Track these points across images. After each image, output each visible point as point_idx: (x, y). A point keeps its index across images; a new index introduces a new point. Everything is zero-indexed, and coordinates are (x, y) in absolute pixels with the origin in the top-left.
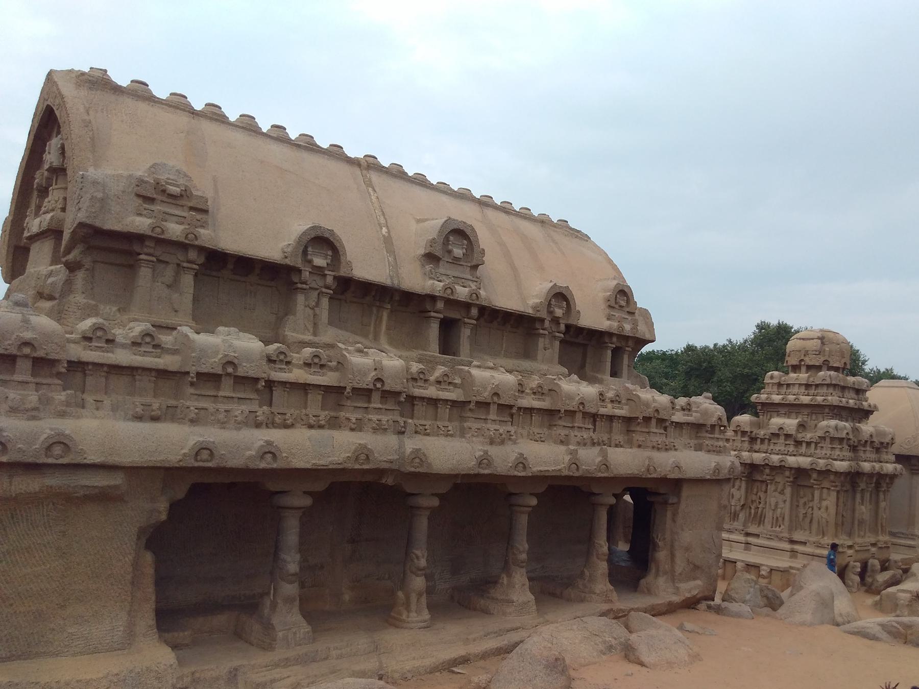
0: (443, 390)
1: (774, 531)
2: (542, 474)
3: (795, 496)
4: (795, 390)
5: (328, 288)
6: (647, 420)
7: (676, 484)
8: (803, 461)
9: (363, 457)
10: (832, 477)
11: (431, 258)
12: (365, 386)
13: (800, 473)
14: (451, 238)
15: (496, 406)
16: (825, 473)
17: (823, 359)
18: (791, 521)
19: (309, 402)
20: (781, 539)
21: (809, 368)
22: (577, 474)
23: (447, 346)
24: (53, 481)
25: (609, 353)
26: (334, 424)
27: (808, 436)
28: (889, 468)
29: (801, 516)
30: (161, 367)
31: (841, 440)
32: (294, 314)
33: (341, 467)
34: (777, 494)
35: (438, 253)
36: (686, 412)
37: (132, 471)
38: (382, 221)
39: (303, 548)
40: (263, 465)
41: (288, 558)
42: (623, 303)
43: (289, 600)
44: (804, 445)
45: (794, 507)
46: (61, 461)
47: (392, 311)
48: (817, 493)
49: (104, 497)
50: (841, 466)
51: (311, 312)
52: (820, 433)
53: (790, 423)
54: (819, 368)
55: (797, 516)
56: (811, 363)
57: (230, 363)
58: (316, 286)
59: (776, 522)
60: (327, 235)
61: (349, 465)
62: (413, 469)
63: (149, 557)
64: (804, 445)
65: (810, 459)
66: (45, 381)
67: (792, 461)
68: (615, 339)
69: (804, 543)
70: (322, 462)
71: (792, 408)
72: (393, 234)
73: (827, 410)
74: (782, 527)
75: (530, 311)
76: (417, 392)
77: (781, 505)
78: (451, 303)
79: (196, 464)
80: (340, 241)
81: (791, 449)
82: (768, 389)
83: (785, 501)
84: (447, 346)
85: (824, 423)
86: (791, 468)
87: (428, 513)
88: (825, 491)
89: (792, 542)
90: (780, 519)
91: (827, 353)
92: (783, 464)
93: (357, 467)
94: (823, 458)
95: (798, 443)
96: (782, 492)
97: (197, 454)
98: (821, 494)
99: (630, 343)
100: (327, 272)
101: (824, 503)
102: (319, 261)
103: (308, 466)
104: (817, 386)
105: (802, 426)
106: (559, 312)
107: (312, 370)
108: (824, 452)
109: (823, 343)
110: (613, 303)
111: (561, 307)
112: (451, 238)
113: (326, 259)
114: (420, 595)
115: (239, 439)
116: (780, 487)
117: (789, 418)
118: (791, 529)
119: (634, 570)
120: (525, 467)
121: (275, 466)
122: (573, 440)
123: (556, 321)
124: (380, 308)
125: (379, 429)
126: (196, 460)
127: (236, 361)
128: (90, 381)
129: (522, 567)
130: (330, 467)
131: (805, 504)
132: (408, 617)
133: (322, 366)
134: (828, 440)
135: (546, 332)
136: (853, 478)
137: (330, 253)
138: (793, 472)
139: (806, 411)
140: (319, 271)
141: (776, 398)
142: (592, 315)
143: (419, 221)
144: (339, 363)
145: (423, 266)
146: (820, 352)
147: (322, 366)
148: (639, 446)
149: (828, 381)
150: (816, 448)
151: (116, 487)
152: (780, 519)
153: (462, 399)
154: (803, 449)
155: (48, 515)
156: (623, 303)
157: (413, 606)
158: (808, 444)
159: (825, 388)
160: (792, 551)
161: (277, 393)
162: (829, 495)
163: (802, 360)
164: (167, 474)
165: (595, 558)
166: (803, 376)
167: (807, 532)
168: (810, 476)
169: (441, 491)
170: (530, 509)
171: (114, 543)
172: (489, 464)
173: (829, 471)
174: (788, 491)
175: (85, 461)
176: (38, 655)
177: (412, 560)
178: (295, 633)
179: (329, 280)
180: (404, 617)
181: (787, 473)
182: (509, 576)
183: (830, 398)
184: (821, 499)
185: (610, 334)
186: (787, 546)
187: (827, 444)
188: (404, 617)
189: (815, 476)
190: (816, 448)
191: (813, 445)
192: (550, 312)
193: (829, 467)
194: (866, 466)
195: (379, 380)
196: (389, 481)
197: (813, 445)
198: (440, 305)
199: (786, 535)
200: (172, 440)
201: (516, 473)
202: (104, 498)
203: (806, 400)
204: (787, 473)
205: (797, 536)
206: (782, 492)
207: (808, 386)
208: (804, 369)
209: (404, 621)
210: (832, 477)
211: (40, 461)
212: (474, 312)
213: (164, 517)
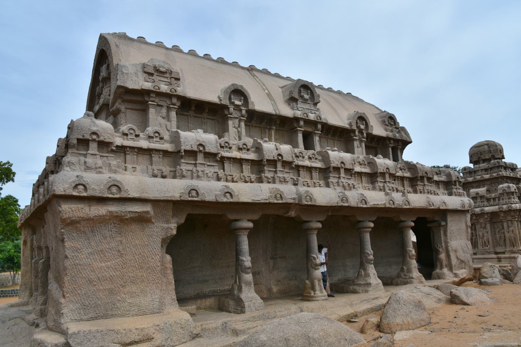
0: (313, 162)
1: (484, 249)
2: (375, 206)
3: (493, 229)
4: (480, 173)
5: (243, 117)
6: (422, 178)
7: (443, 213)
9: (279, 196)
10: (512, 214)
12: (272, 158)
13: (493, 214)
14: (302, 89)
15: (343, 169)
17: (491, 155)
18: (493, 242)
19: (244, 170)
20: (489, 253)
21: (484, 161)
22: (393, 207)
23: (308, 145)
24: (114, 208)
25: (390, 149)
29: (498, 239)
30: (165, 149)
32: (228, 131)
33: (267, 201)
34: (482, 229)
35: (296, 96)
36: (439, 175)
37: (155, 203)
38: (264, 87)
39: (251, 252)
40: (225, 200)
41: (244, 259)
42: (392, 123)
43: (248, 284)
44: (492, 200)
45: (494, 234)
46: (116, 196)
47: (276, 130)
48: (505, 225)
49: (142, 220)
51: (236, 130)
52: (500, 192)
53: (482, 190)
54: (489, 160)
55: (496, 239)
56: (484, 158)
57: (201, 145)
58: (237, 116)
59: (485, 244)
60: (240, 88)
61: (272, 201)
62: (306, 203)
63: (168, 257)
64: (492, 200)
65: (497, 207)
66: (104, 155)
67: (487, 209)
68: (392, 142)
69: (504, 253)
70: (257, 199)
72: (271, 92)
73: (500, 180)
74: (489, 246)
76: (301, 163)
77: (486, 235)
78: (308, 122)
79: (190, 199)
80: (246, 91)
81: (486, 203)
83: (487, 232)
85: (501, 186)
86: (487, 213)
87: (316, 232)
88: (509, 222)
89: (496, 253)
90: (487, 242)
91: (492, 151)
92: (483, 211)
93: (276, 201)
94: (505, 204)
95: (488, 200)
96: (485, 228)
97: (189, 193)
98: (508, 224)
99: (400, 143)
100: (242, 108)
101: (511, 229)
102: (237, 102)
103: (250, 201)
104: (491, 169)
105: (488, 190)
106: (362, 127)
107: (244, 151)
108: (504, 201)
109: (489, 147)
110: (387, 123)
111: (363, 124)
112: (302, 89)
113: (241, 101)
114: (319, 281)
115: (210, 187)
116: (483, 225)
117: (479, 188)
118: (494, 247)
120: (366, 203)
121: (232, 200)
122: (387, 188)
123: (361, 131)
124: (270, 129)
125: (284, 181)
126: (189, 197)
127: (203, 144)
128: (128, 157)
129: (371, 264)
130: (262, 201)
131: (499, 231)
132: (314, 294)
133: (248, 150)
134: (505, 194)
135: (357, 138)
137: (242, 98)
138: (489, 215)
140: (237, 108)
142: (378, 130)
144: (256, 148)
145: (289, 104)
147: (248, 150)
148: (421, 192)
149: (497, 165)
150: (499, 200)
151: (147, 212)
152: (487, 242)
153: (324, 167)
154: (492, 202)
155: (111, 231)
156: (392, 123)
157: (317, 287)
158: (494, 199)
159: (496, 168)
160: (498, 258)
161: (226, 165)
162: (512, 224)
163: (479, 158)
164: (176, 205)
165: (408, 259)
166: (483, 165)
167: (503, 247)
168: (499, 216)
169: (321, 220)
170: (371, 229)
171: (149, 245)
172: (347, 200)
173: (510, 210)
174: (488, 226)
175: (129, 196)
176: (113, 316)
177: (311, 261)
178: (254, 303)
179: (244, 112)
180: (312, 294)
181: (486, 216)
182: (365, 270)
183: (500, 173)
184: (508, 227)
186: (494, 256)
187: (506, 196)
188: (312, 294)
189: (502, 215)
190: (499, 200)
191: (497, 199)
192: (358, 127)
193: (510, 208)
195: (279, 155)
196: (293, 214)
197: (497, 199)
198: (302, 123)
199: (492, 250)
200: (174, 188)
201: (362, 206)
202: (142, 220)
203: (487, 176)
204: (486, 216)
205: (499, 250)
206: (485, 228)
207: (486, 170)
208: (481, 162)
209: (313, 297)
210: (512, 214)
211: (105, 196)
212: (319, 126)
213: (174, 232)
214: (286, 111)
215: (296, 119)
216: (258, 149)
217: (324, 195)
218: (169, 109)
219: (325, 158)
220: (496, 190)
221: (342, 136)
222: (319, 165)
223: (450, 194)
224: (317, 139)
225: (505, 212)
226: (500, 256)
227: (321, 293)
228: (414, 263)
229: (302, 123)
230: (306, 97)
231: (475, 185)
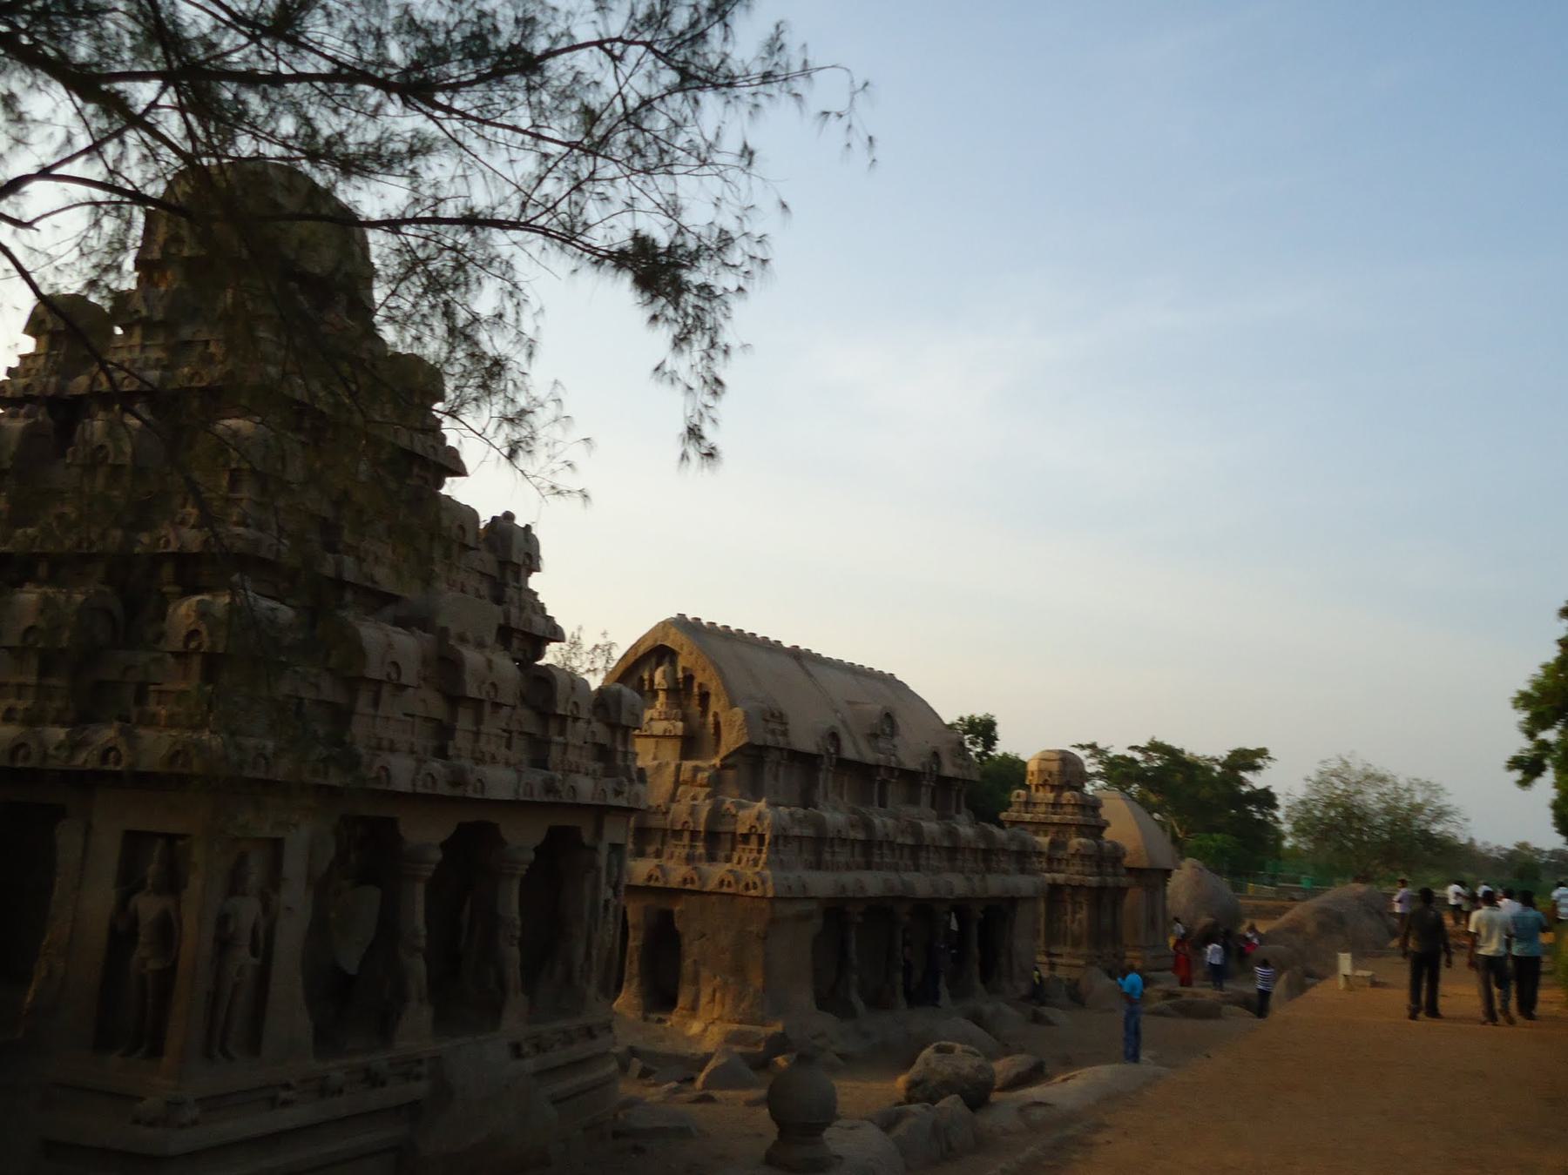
7: (1013, 901)
8: (1060, 878)
11: (875, 736)
16: (1077, 889)
26: (868, 866)
27: (1060, 854)
28: (1124, 881)
31: (1090, 857)
48: (1069, 908)
50: (1093, 881)
71: (1040, 826)
75: (919, 768)
78: (890, 770)
82: (1015, 808)
84: (882, 804)
89: (1049, 955)
105: (1053, 844)
119: (987, 972)
136: (1101, 889)
139: (1055, 829)
141: (1027, 817)
143: (849, 703)
146: (1062, 772)
154: (1055, 865)
158: (1059, 860)
184: (1074, 913)
185: (956, 779)
187: (1077, 861)
194: (1110, 881)
200: (823, 883)
203: (1056, 818)
205: (1054, 950)
214: (870, 757)
215: (878, 766)
216: (868, 826)
217: (921, 884)
218: (779, 764)
219: (916, 831)
220: (1064, 846)
221: (911, 778)
222: (910, 841)
223: (1023, 871)
224: (890, 788)
225: (1074, 887)
226: (1055, 960)
227: (901, 1001)
228: (976, 969)
229: (882, 771)
230: (888, 730)
231: (1031, 828)
